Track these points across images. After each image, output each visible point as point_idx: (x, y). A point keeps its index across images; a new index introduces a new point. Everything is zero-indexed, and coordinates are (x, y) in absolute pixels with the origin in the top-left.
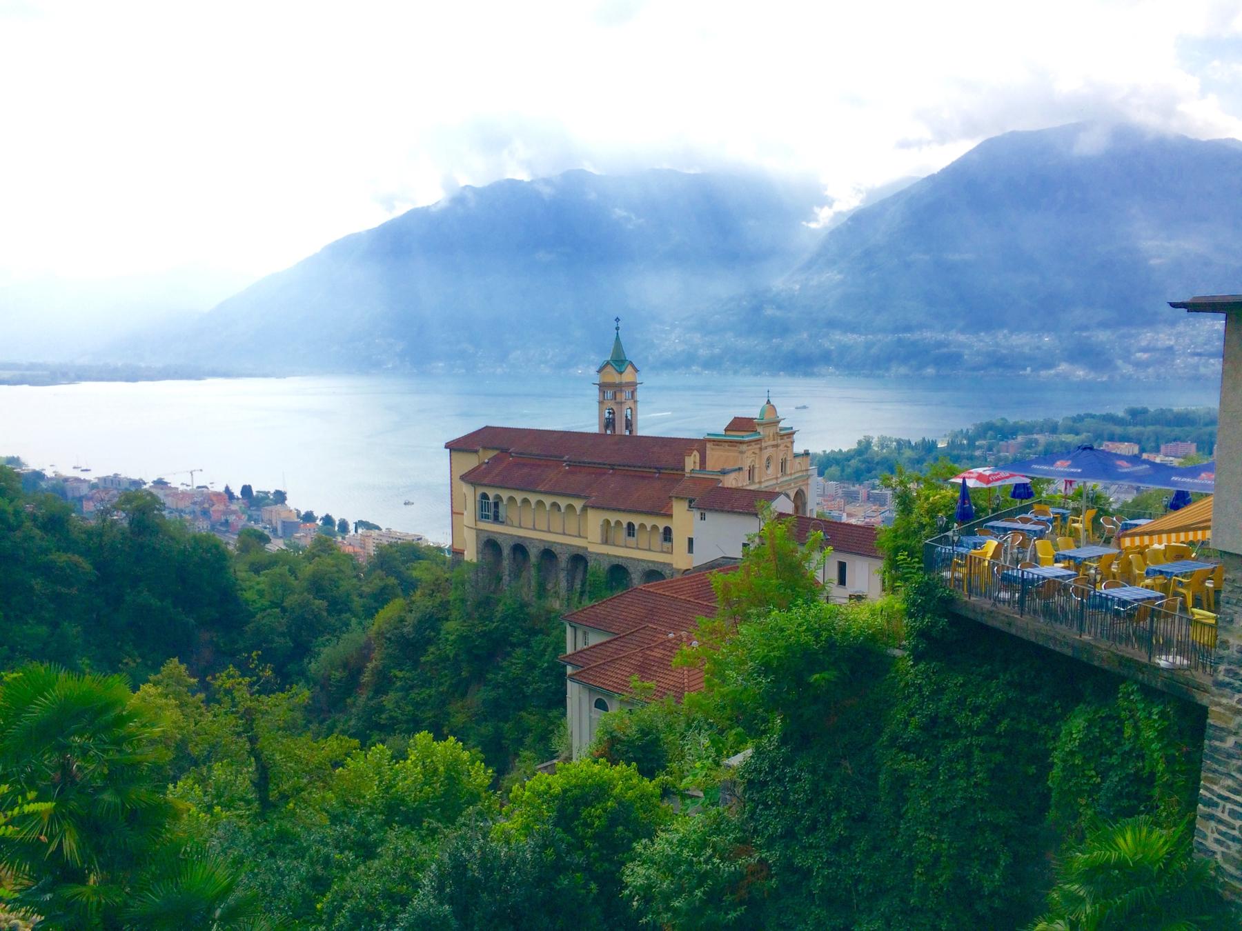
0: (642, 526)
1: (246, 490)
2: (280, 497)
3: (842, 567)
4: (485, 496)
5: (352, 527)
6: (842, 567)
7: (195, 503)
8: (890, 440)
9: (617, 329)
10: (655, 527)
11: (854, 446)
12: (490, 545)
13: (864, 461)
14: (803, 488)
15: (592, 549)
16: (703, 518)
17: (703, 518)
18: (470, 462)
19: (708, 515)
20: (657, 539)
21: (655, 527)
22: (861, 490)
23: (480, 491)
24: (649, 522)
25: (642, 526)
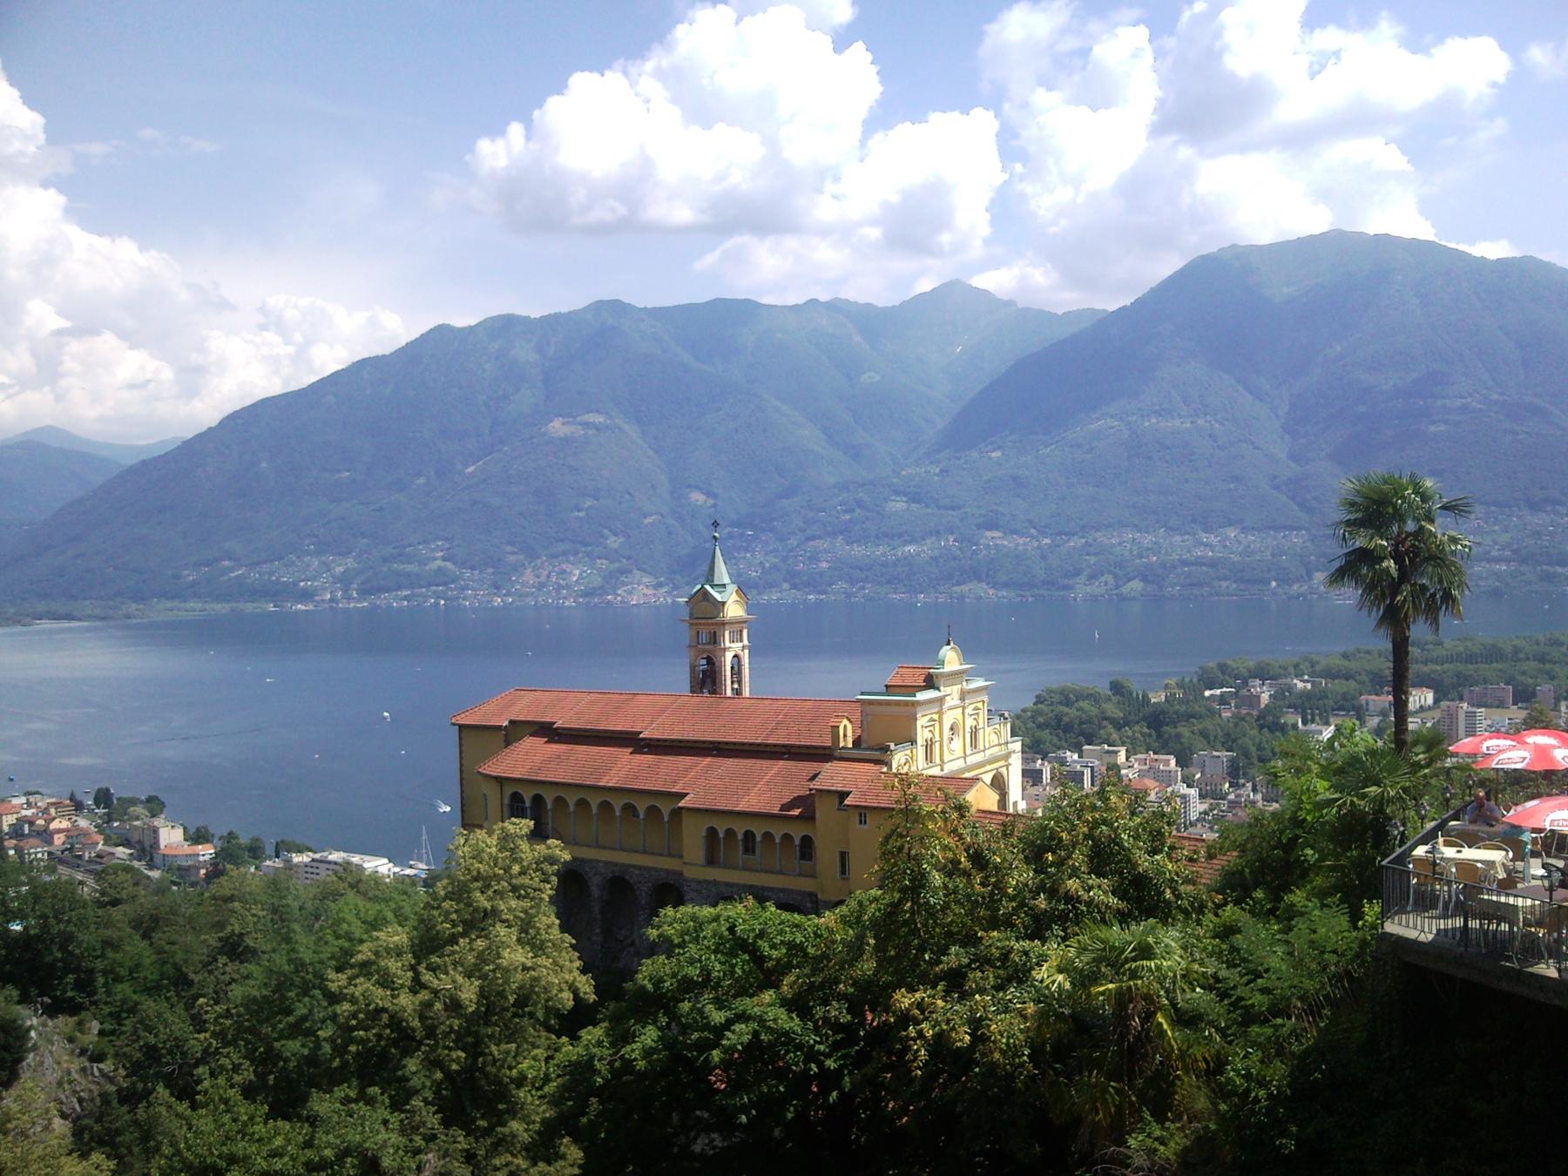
0: (768, 836)
14: (1004, 770)
15: (689, 873)
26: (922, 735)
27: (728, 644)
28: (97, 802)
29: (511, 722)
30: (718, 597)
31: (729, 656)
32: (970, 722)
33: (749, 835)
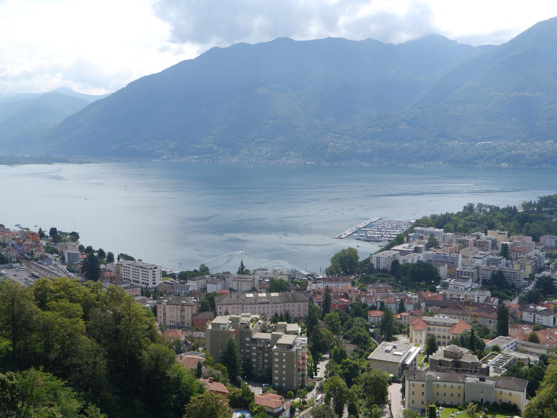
1: (53, 231)
2: (75, 236)
5: (116, 257)
7: (14, 239)
8: (486, 206)
11: (461, 210)
13: (470, 220)
22: (471, 239)
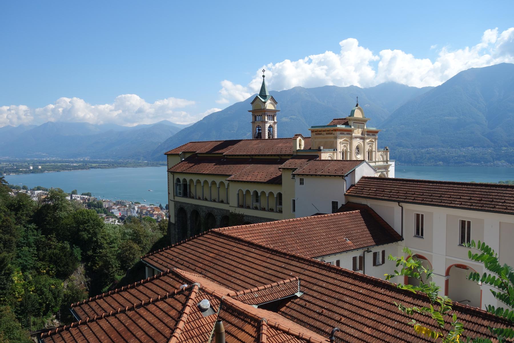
0: (263, 193)
3: (419, 219)
4: (178, 180)
6: (419, 219)
9: (264, 76)
10: (271, 194)
12: (181, 211)
15: (232, 210)
16: (302, 183)
17: (302, 183)
18: (176, 160)
19: (306, 180)
20: (272, 203)
21: (271, 194)
23: (177, 176)
24: (268, 189)
25: (263, 193)
26: (340, 147)
27: (266, 120)
28: (166, 207)
29: (183, 152)
30: (263, 100)
31: (267, 125)
32: (367, 148)
33: (256, 193)
